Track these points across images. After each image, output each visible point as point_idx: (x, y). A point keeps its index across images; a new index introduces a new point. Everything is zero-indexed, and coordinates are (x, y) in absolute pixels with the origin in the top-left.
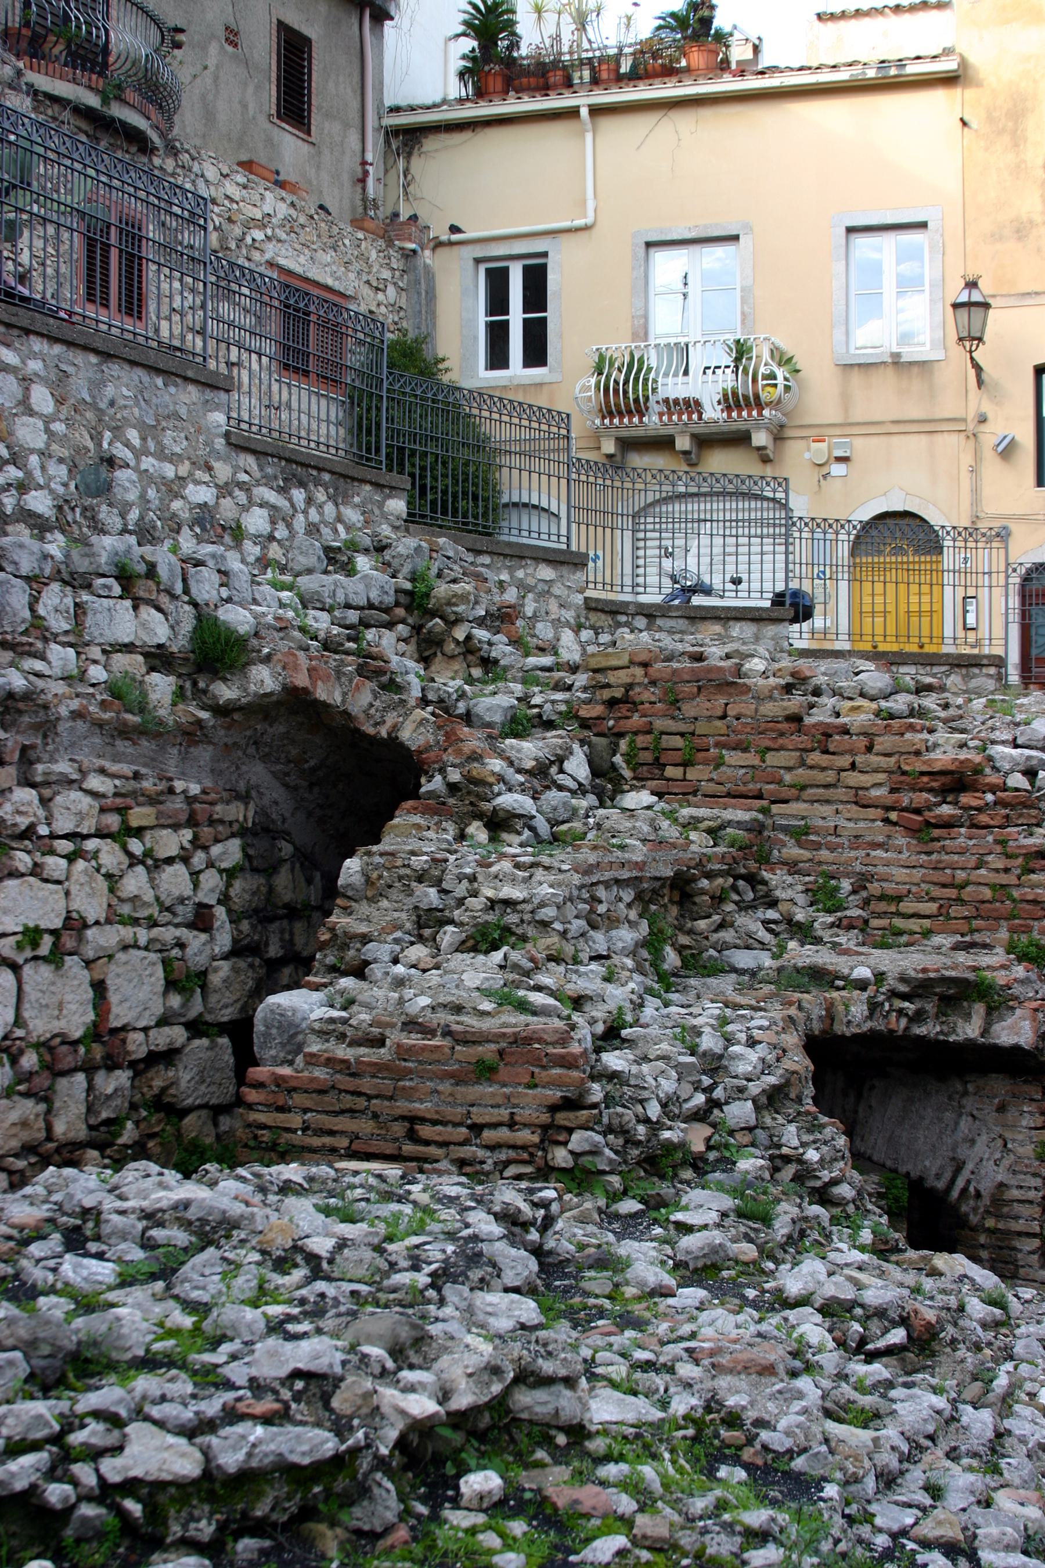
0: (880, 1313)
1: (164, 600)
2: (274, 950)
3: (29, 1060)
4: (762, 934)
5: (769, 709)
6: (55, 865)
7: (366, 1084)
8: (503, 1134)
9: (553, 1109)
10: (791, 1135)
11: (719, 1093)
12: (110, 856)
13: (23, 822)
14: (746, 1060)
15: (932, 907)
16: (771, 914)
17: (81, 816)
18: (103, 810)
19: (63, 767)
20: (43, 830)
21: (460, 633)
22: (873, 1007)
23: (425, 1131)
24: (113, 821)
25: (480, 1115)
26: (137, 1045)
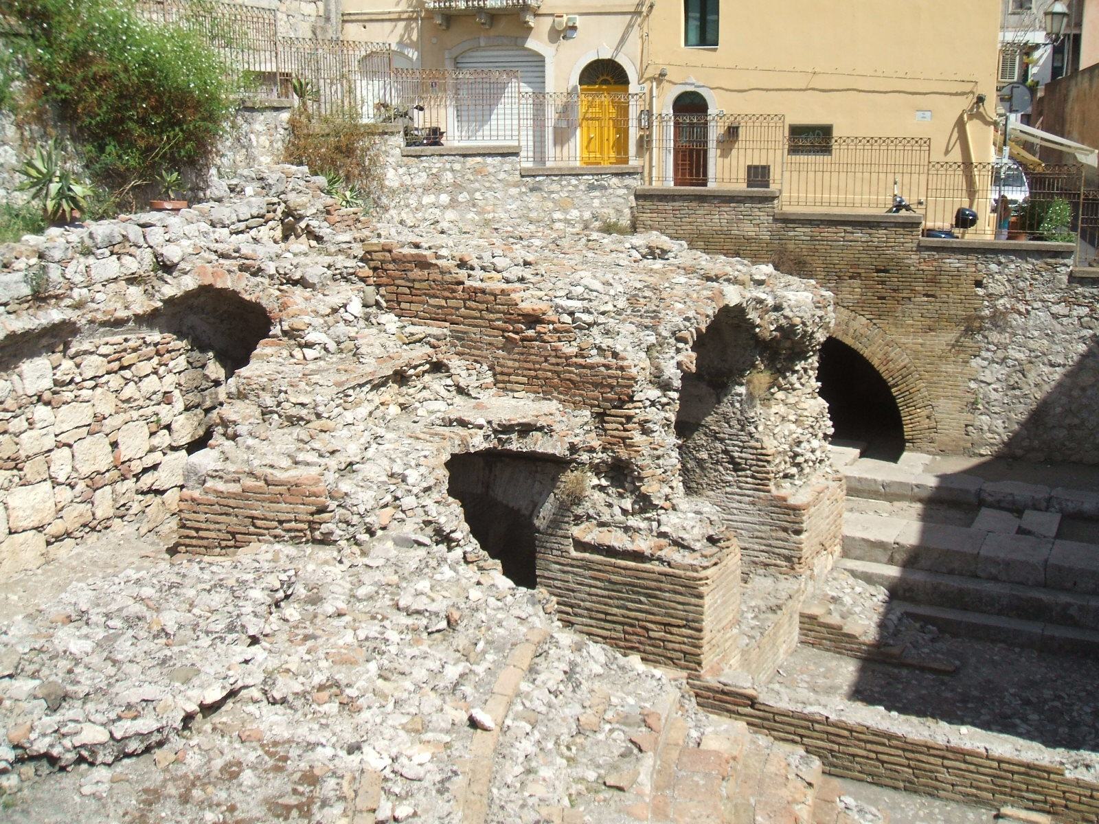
0: (437, 614)
1: (133, 250)
2: (208, 404)
3: (81, 486)
4: (443, 393)
5: (447, 277)
6: (85, 394)
7: (232, 502)
8: (293, 524)
9: (312, 514)
10: (433, 509)
11: (399, 494)
12: (115, 381)
13: (68, 378)
14: (413, 476)
15: (525, 380)
16: (449, 382)
17: (98, 367)
18: (109, 362)
19: (87, 346)
20: (78, 379)
21: (303, 224)
22: (486, 437)
23: (259, 523)
24: (116, 365)
25: (283, 517)
26: (137, 467)
